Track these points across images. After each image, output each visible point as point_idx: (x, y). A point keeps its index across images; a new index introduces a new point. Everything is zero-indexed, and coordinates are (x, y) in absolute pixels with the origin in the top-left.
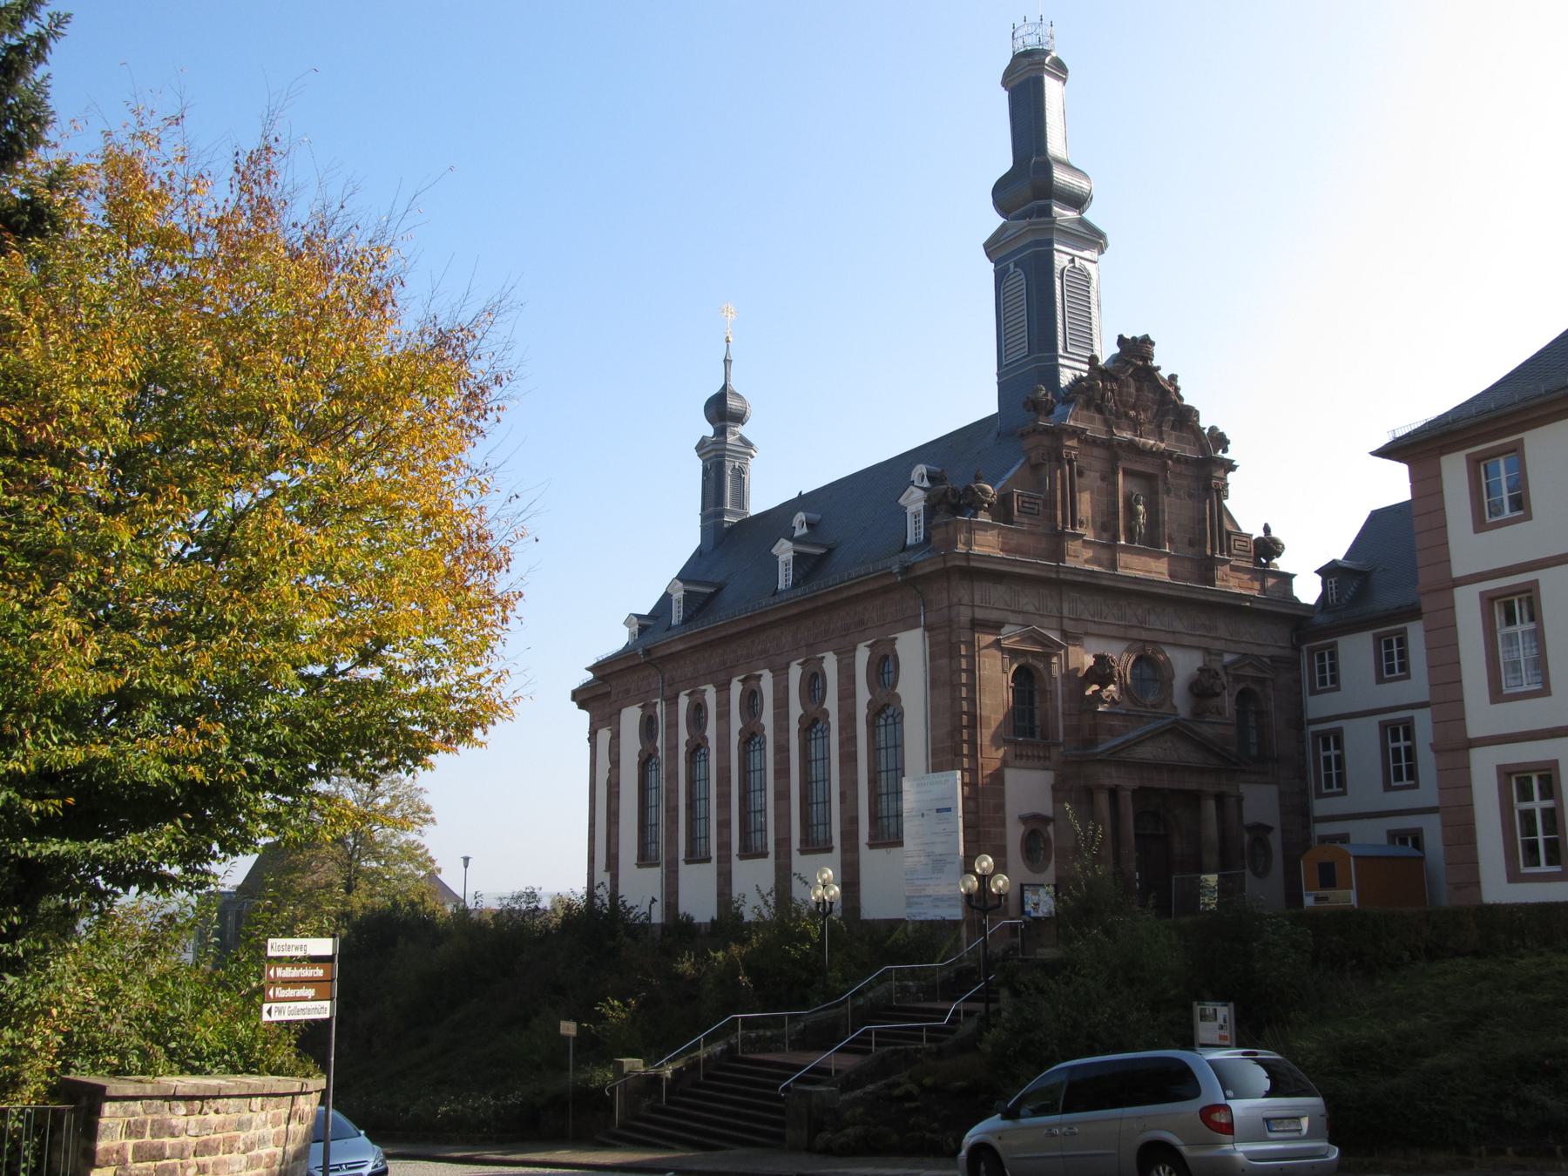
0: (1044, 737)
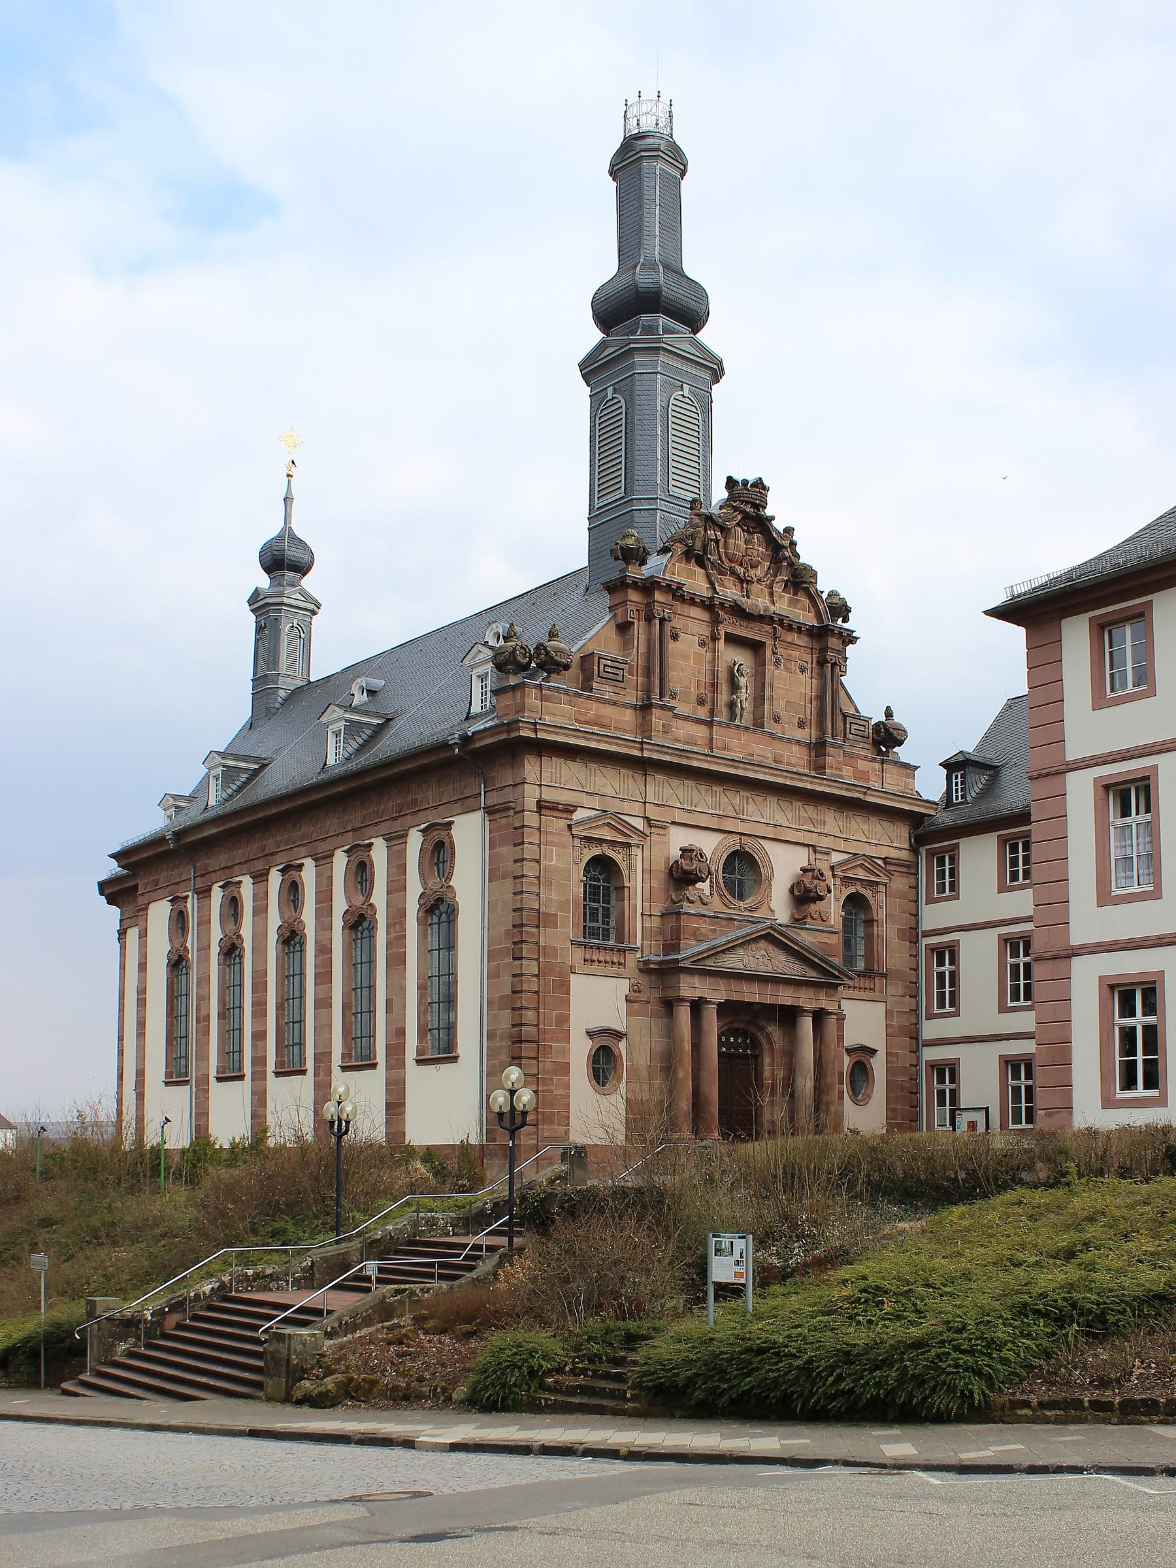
0: (620, 939)
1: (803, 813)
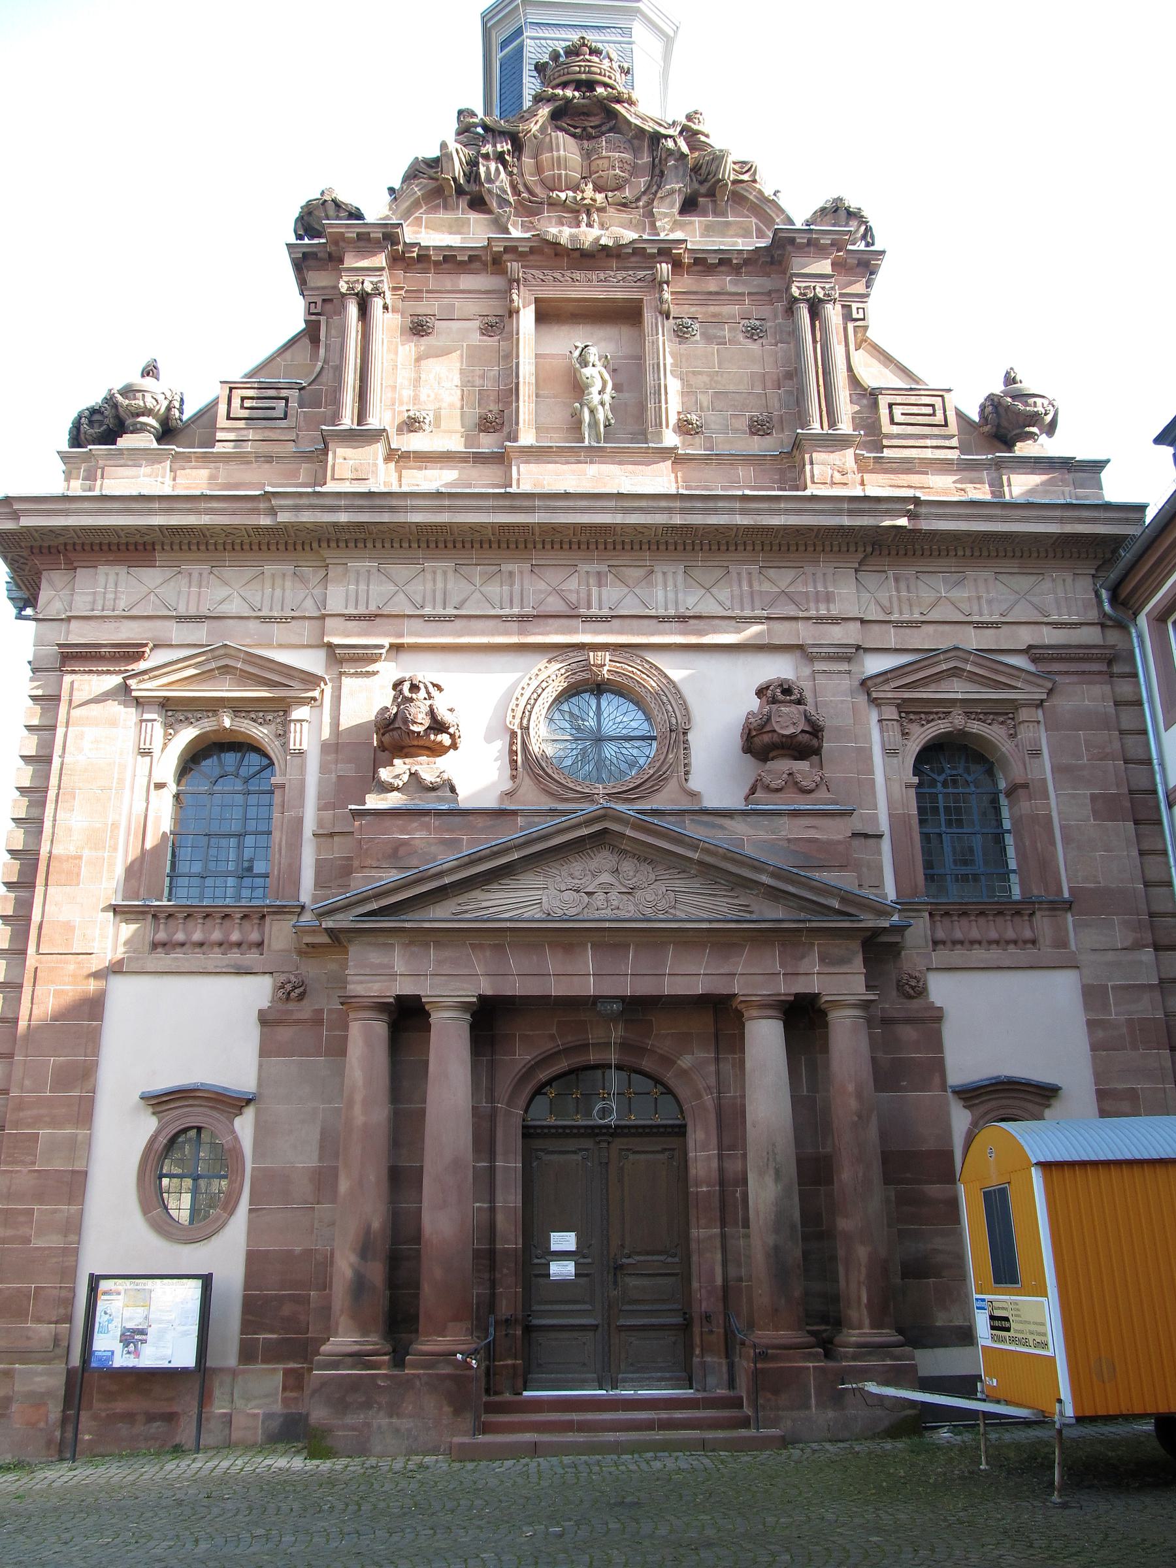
1: (767, 587)
